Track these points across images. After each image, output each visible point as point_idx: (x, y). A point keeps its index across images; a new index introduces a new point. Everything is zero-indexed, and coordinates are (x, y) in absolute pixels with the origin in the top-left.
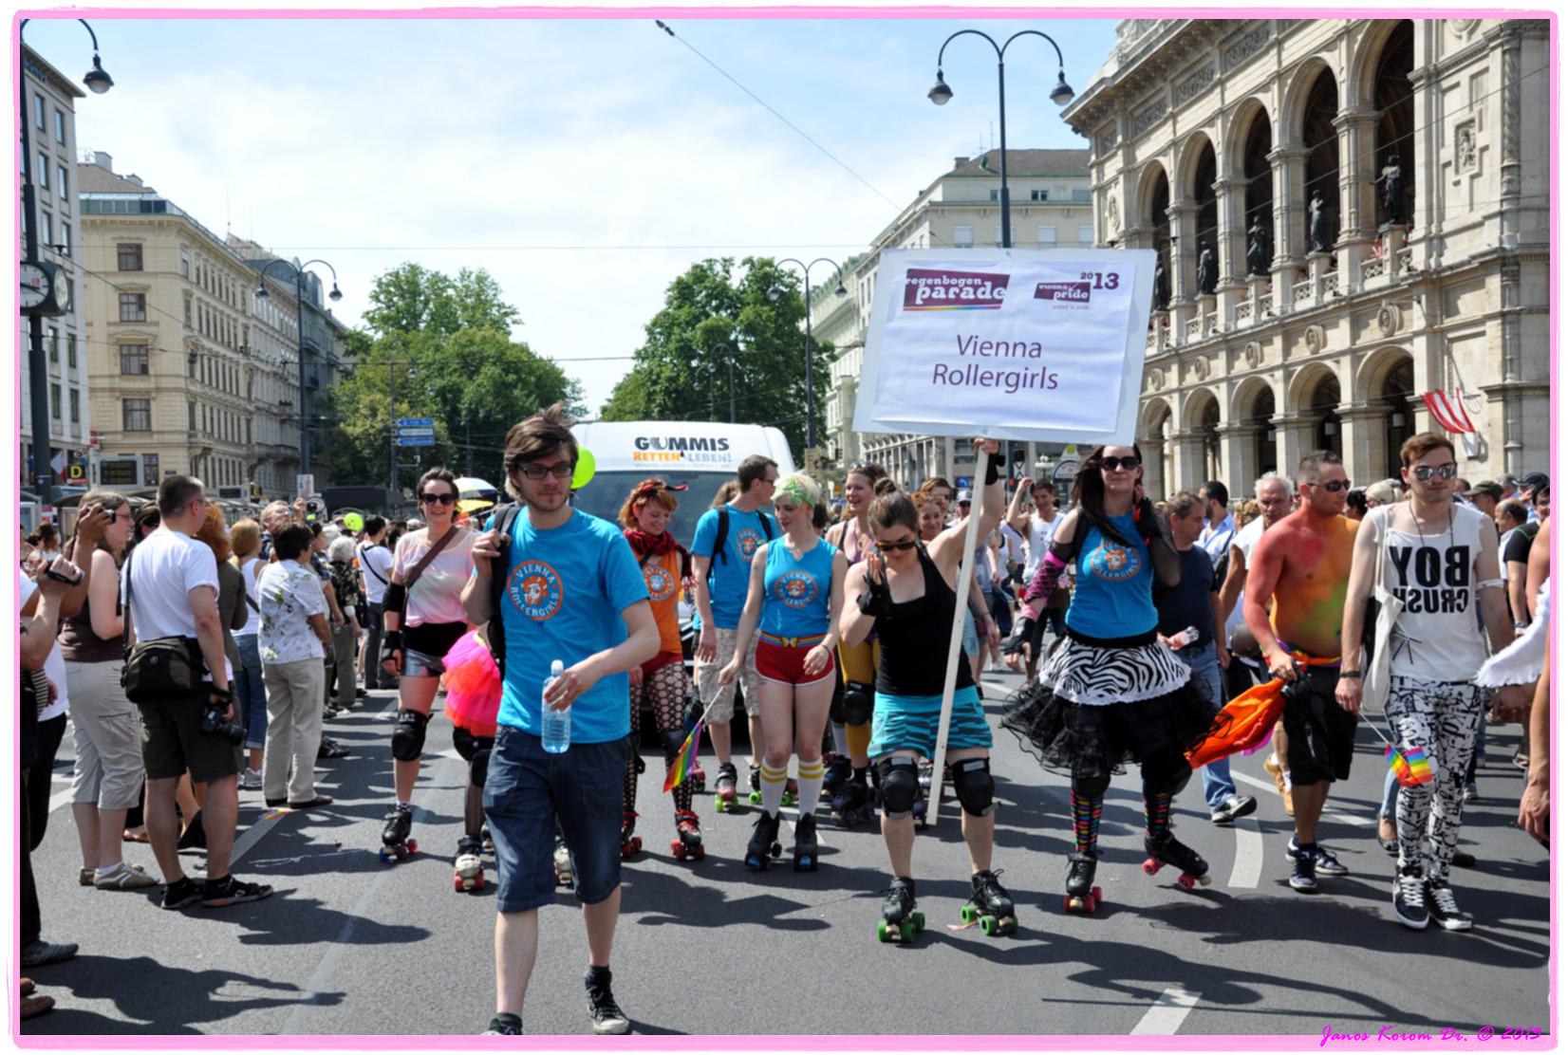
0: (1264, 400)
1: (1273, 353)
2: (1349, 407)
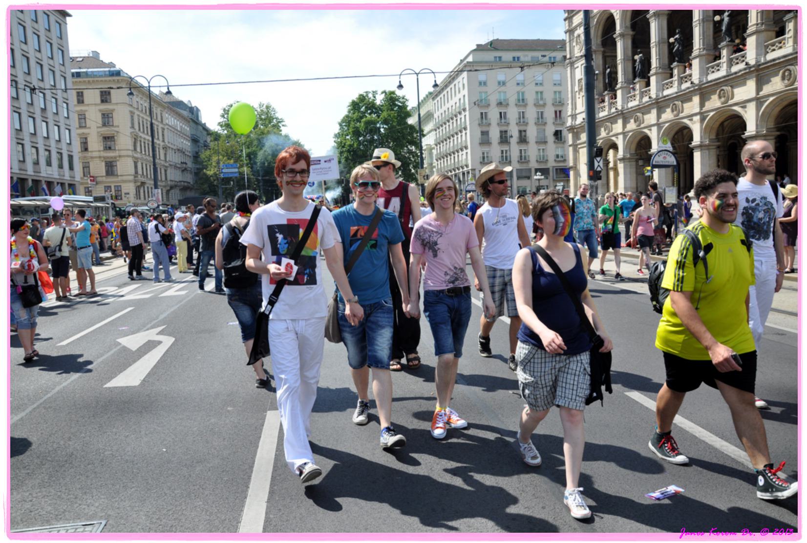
0: (644, 143)
1: (693, 106)
2: (754, 133)
